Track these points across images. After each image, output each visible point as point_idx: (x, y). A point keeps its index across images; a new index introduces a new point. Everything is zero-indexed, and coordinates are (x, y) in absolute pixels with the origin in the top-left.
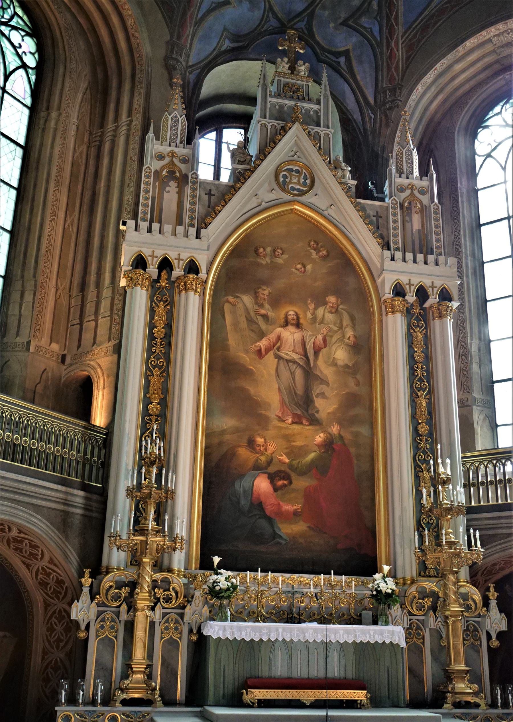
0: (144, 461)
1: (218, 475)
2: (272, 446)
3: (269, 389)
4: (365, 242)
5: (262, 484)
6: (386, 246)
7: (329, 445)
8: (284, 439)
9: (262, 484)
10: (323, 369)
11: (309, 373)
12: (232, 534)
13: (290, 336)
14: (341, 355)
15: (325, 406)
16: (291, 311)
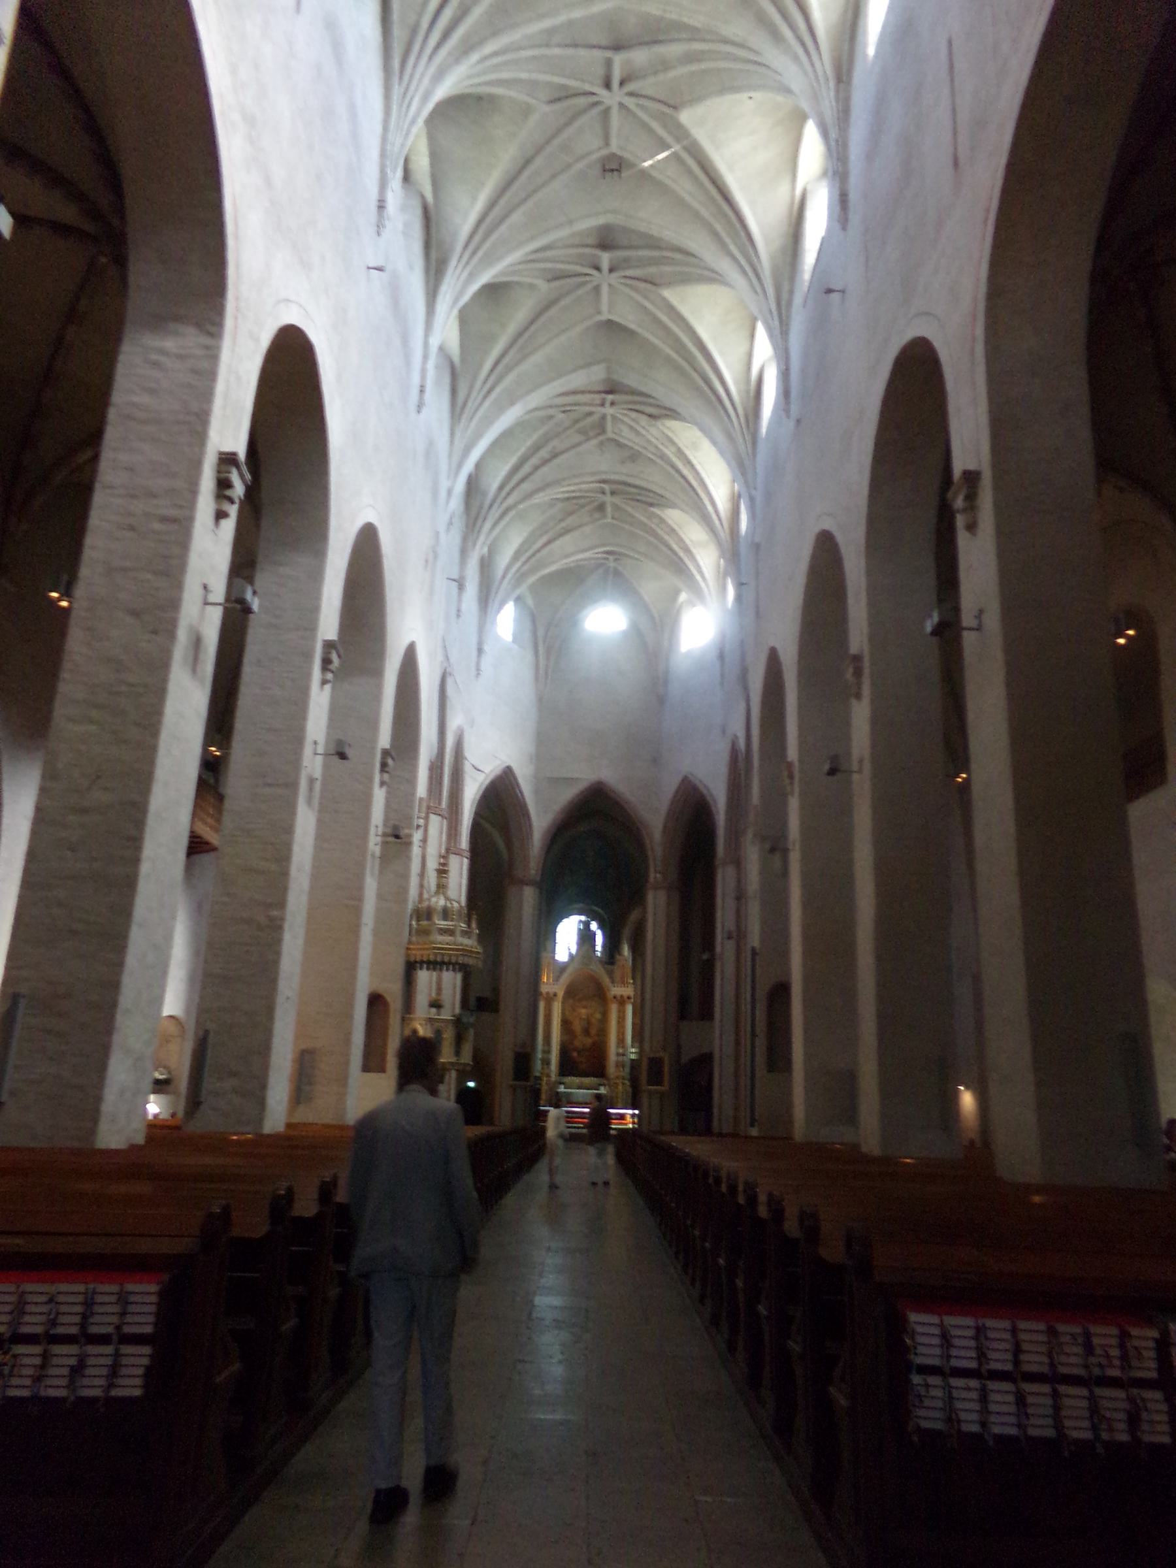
0: (544, 1052)
1: (564, 1052)
2: (577, 1043)
3: (577, 1027)
4: (606, 980)
5: (575, 1054)
6: (613, 982)
7: (594, 1044)
8: (581, 1041)
9: (575, 1054)
10: (593, 1020)
11: (589, 1023)
12: (568, 1067)
13: (583, 1011)
14: (598, 1016)
15: (593, 1032)
16: (584, 1003)
